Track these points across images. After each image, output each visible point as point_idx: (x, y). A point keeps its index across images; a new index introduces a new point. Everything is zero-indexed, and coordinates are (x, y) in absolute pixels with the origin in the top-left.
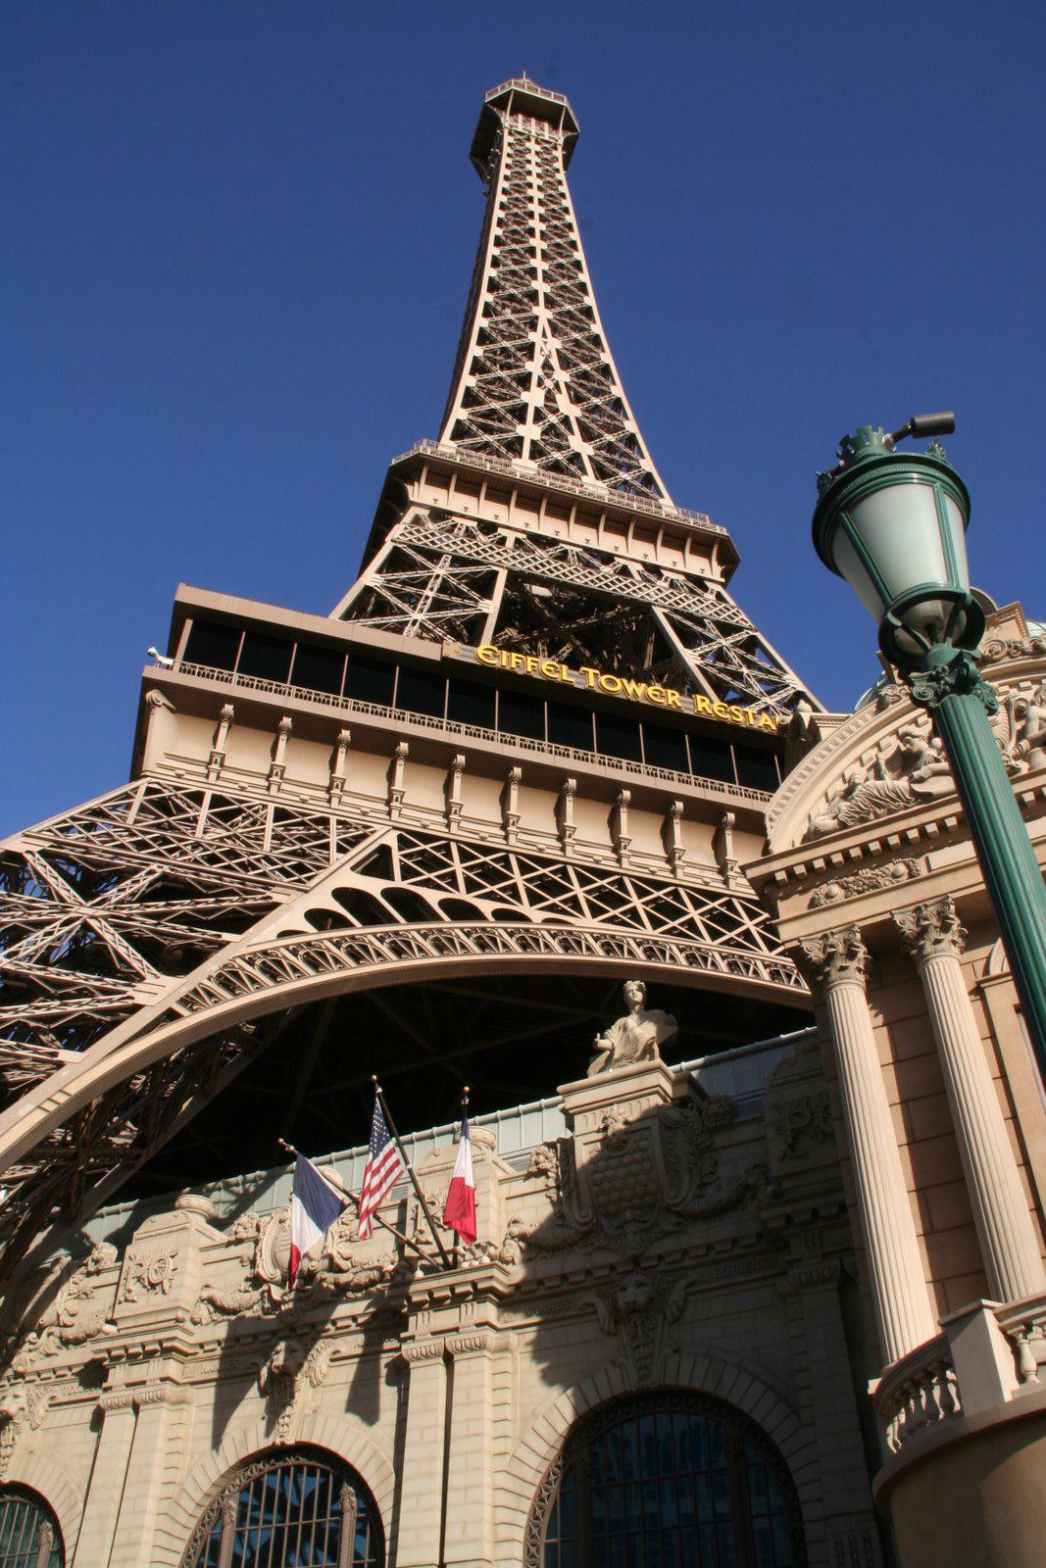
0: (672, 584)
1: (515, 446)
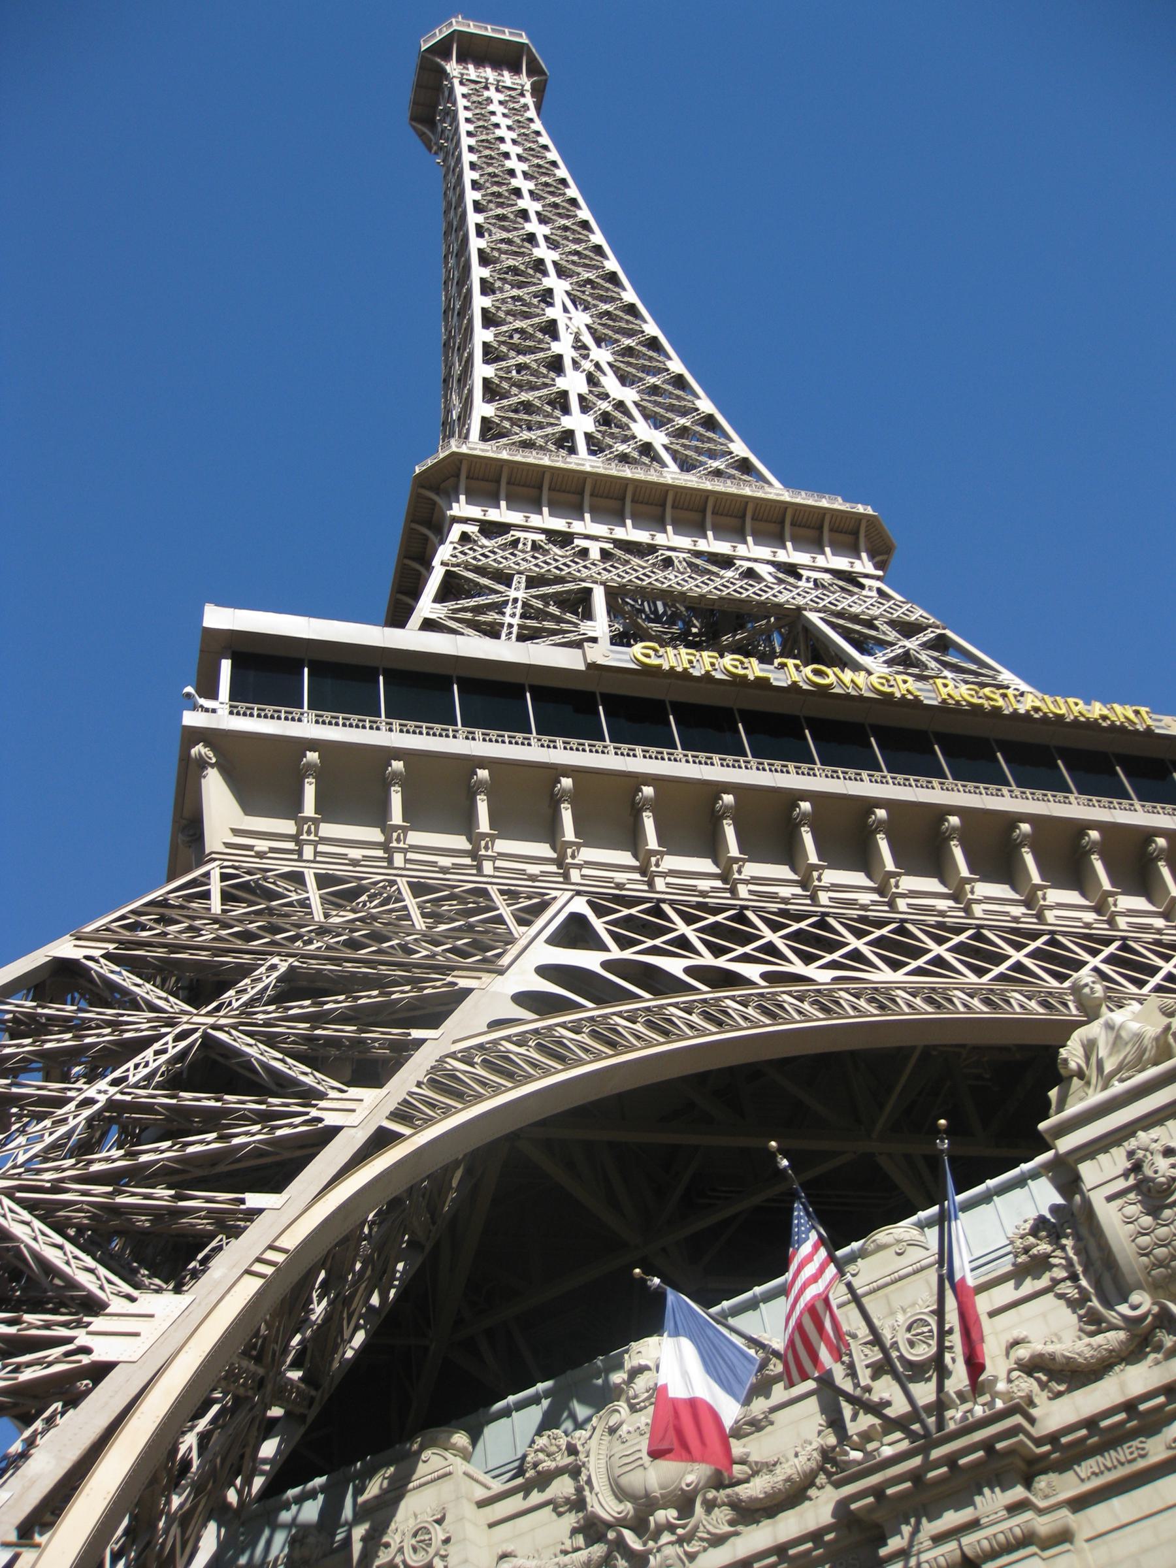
0: (817, 584)
1: (566, 440)
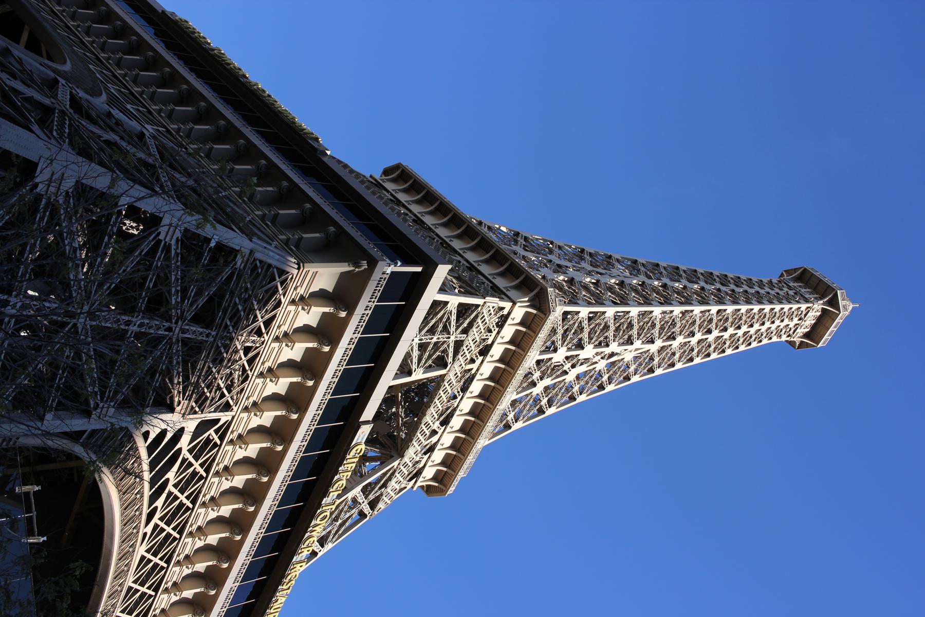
1: (552, 348)
